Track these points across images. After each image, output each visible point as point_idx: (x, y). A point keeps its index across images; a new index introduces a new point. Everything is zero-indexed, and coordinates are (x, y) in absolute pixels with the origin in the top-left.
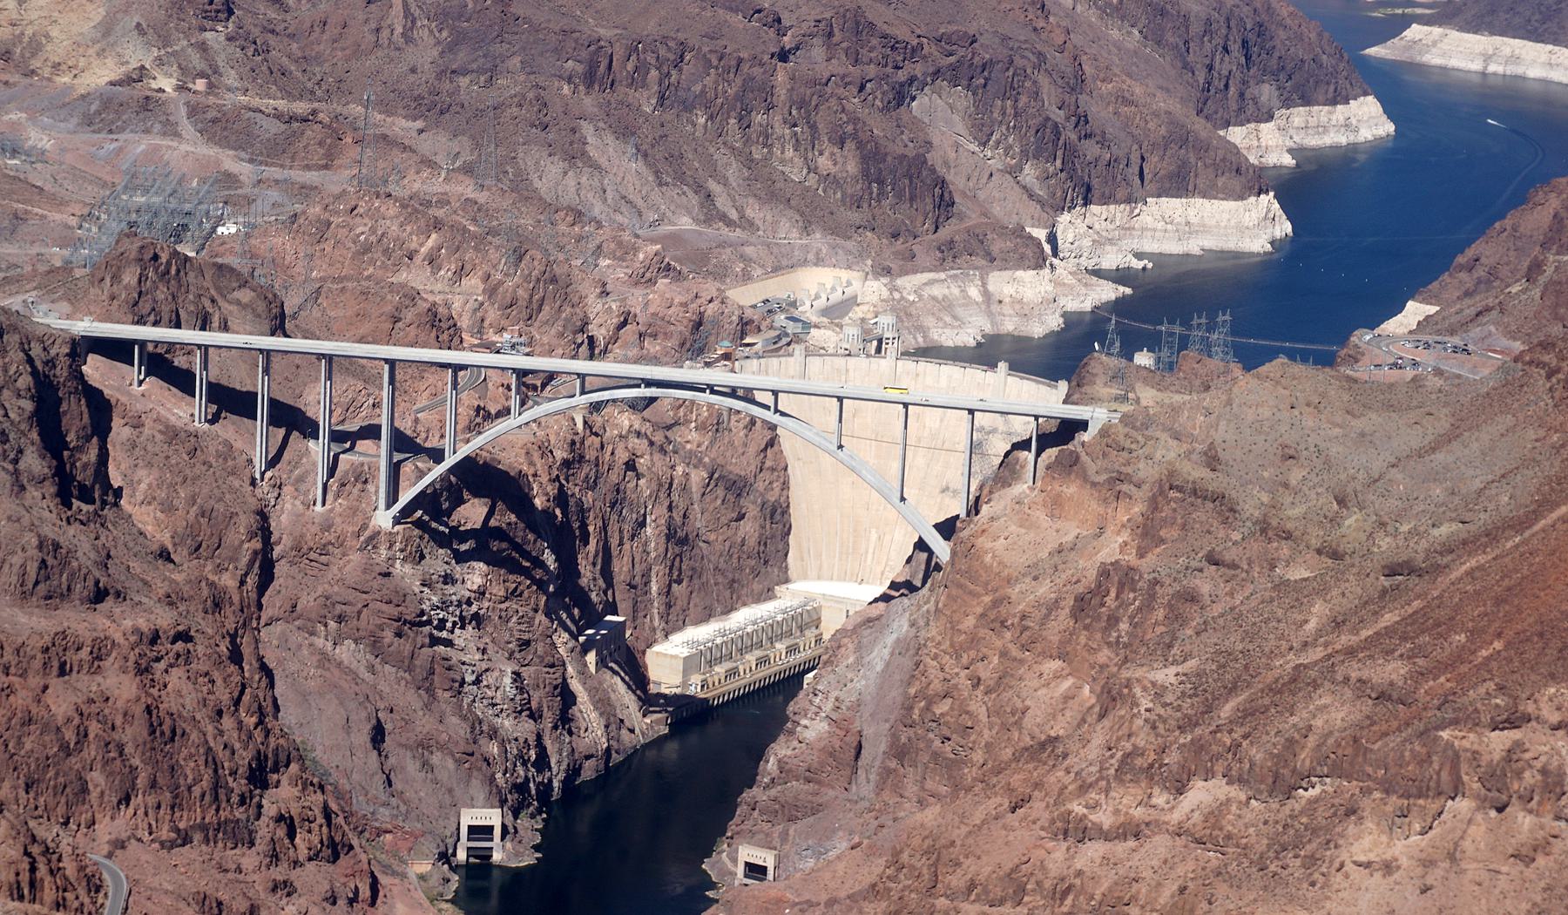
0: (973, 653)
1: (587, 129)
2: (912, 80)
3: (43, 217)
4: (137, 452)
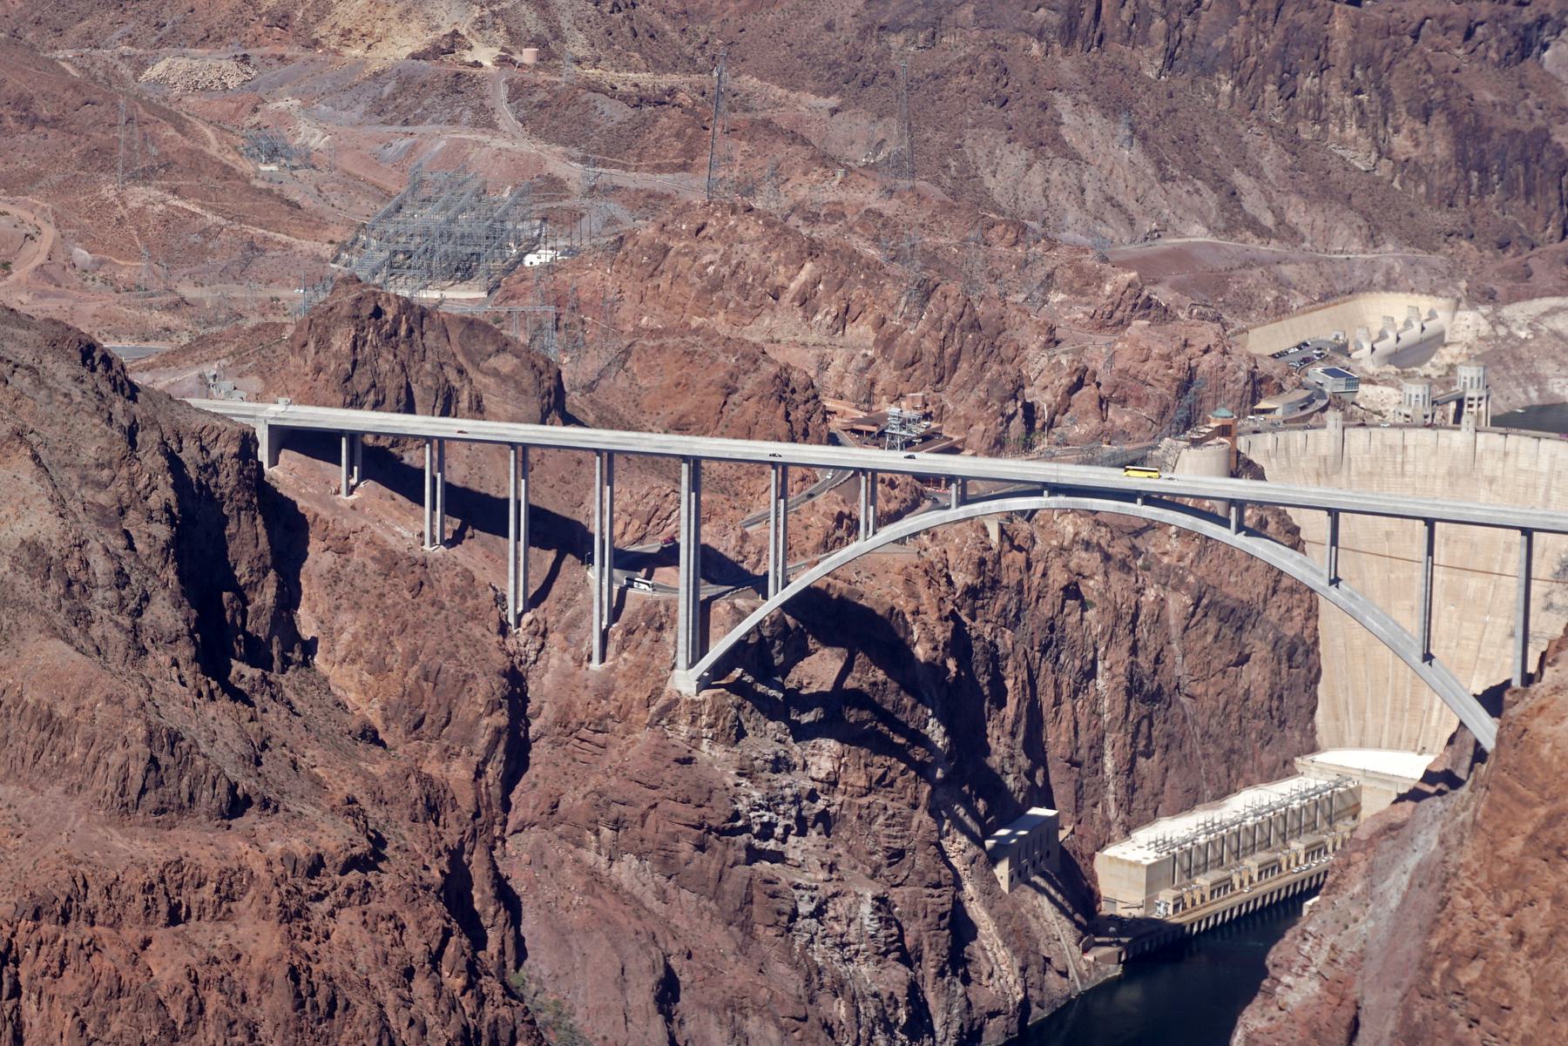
0: (1517, 894)
1: (1063, 104)
2: (1542, 21)
3: (287, 246)
4: (342, 588)
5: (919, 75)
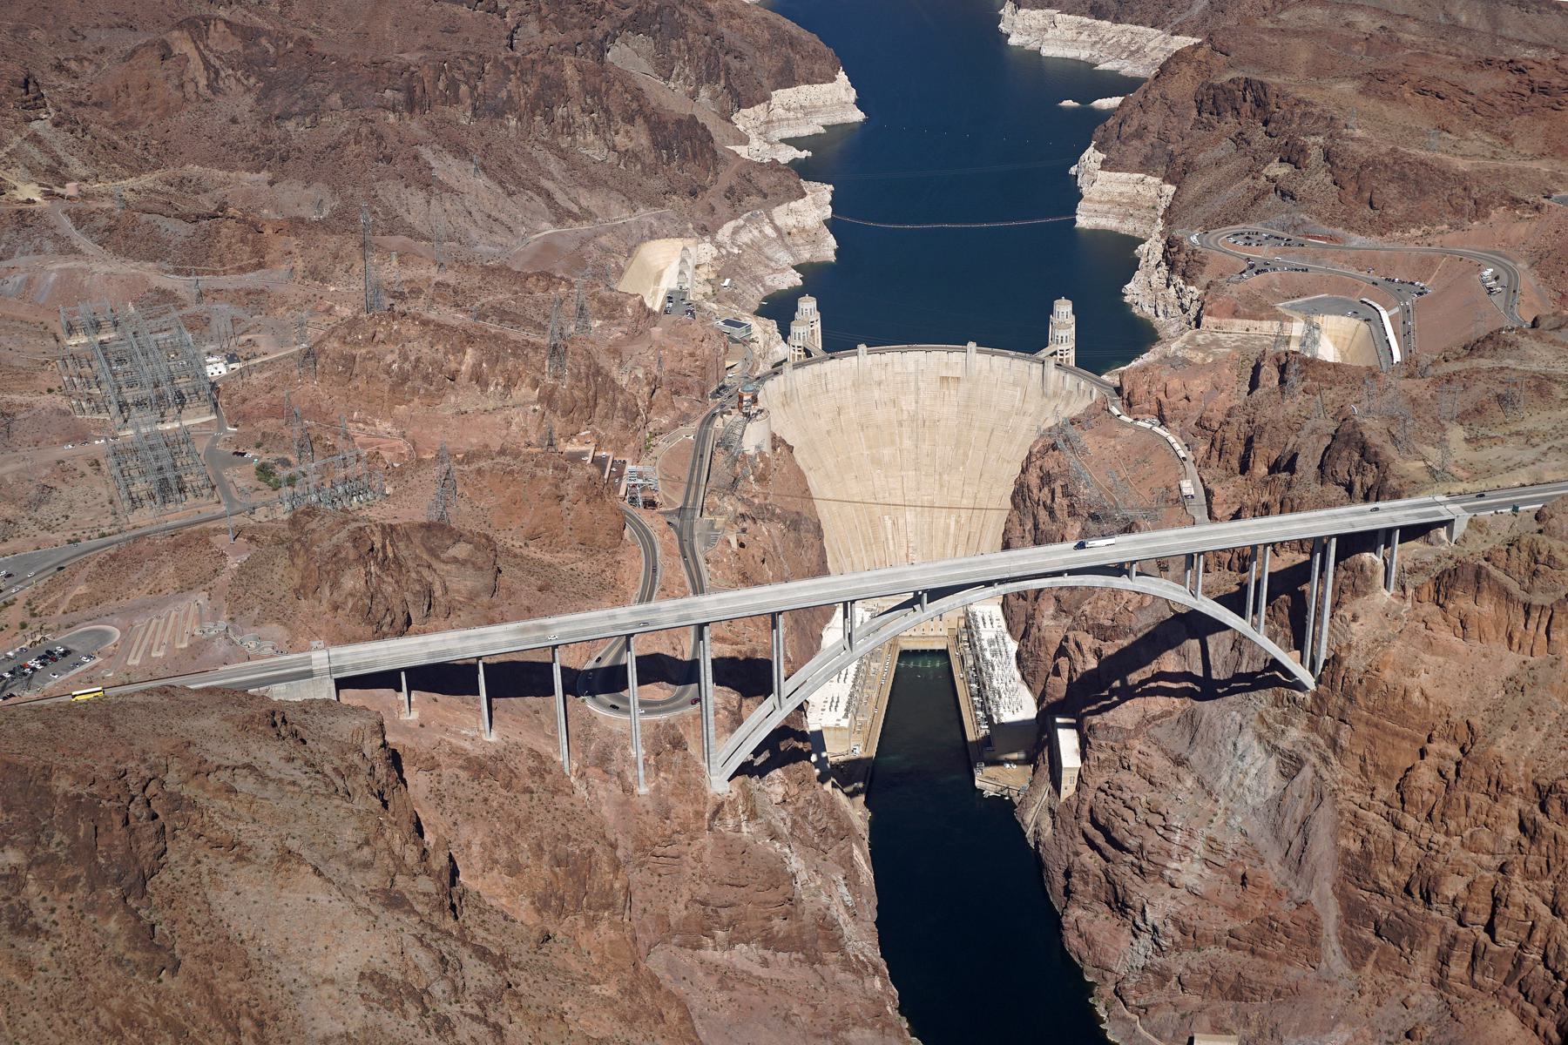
1: (427, 154)
4: (449, 804)
5: (319, 148)
